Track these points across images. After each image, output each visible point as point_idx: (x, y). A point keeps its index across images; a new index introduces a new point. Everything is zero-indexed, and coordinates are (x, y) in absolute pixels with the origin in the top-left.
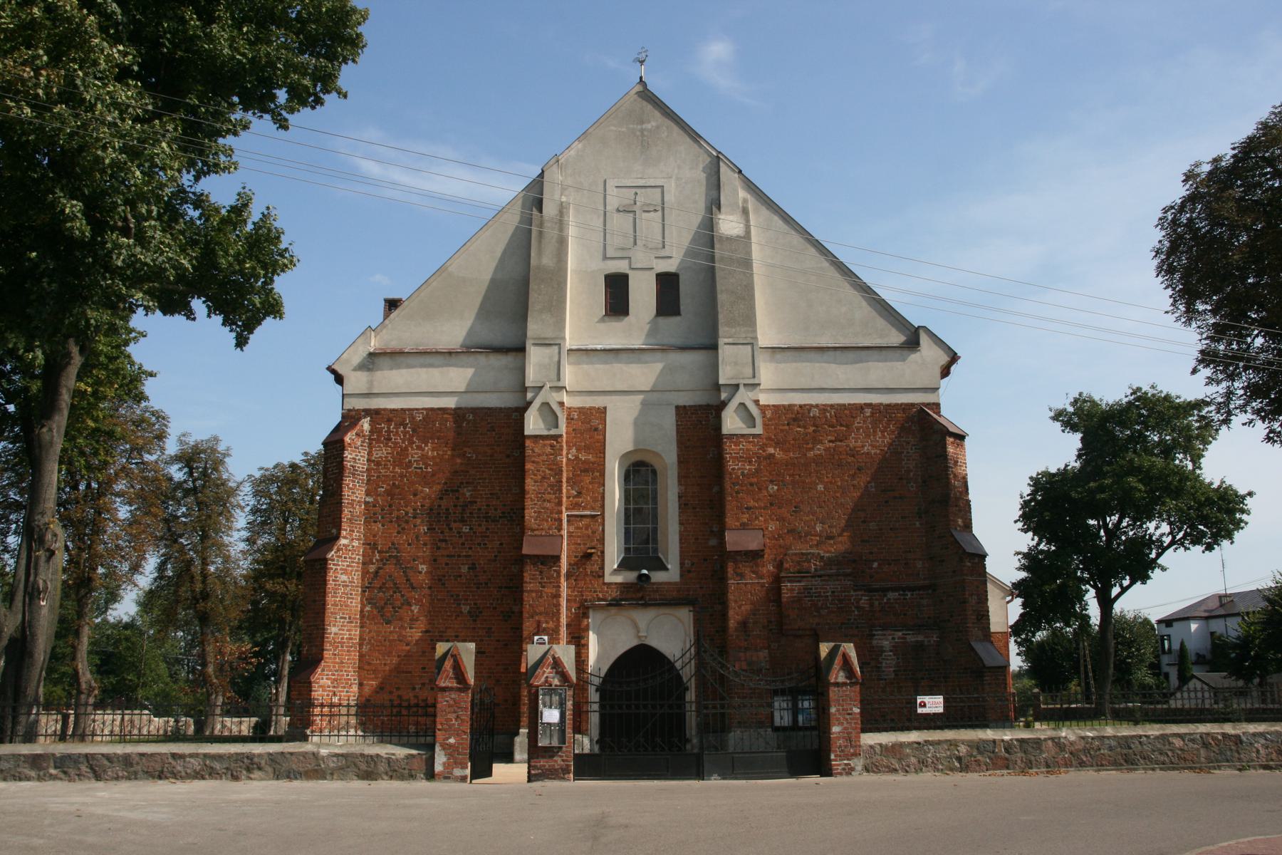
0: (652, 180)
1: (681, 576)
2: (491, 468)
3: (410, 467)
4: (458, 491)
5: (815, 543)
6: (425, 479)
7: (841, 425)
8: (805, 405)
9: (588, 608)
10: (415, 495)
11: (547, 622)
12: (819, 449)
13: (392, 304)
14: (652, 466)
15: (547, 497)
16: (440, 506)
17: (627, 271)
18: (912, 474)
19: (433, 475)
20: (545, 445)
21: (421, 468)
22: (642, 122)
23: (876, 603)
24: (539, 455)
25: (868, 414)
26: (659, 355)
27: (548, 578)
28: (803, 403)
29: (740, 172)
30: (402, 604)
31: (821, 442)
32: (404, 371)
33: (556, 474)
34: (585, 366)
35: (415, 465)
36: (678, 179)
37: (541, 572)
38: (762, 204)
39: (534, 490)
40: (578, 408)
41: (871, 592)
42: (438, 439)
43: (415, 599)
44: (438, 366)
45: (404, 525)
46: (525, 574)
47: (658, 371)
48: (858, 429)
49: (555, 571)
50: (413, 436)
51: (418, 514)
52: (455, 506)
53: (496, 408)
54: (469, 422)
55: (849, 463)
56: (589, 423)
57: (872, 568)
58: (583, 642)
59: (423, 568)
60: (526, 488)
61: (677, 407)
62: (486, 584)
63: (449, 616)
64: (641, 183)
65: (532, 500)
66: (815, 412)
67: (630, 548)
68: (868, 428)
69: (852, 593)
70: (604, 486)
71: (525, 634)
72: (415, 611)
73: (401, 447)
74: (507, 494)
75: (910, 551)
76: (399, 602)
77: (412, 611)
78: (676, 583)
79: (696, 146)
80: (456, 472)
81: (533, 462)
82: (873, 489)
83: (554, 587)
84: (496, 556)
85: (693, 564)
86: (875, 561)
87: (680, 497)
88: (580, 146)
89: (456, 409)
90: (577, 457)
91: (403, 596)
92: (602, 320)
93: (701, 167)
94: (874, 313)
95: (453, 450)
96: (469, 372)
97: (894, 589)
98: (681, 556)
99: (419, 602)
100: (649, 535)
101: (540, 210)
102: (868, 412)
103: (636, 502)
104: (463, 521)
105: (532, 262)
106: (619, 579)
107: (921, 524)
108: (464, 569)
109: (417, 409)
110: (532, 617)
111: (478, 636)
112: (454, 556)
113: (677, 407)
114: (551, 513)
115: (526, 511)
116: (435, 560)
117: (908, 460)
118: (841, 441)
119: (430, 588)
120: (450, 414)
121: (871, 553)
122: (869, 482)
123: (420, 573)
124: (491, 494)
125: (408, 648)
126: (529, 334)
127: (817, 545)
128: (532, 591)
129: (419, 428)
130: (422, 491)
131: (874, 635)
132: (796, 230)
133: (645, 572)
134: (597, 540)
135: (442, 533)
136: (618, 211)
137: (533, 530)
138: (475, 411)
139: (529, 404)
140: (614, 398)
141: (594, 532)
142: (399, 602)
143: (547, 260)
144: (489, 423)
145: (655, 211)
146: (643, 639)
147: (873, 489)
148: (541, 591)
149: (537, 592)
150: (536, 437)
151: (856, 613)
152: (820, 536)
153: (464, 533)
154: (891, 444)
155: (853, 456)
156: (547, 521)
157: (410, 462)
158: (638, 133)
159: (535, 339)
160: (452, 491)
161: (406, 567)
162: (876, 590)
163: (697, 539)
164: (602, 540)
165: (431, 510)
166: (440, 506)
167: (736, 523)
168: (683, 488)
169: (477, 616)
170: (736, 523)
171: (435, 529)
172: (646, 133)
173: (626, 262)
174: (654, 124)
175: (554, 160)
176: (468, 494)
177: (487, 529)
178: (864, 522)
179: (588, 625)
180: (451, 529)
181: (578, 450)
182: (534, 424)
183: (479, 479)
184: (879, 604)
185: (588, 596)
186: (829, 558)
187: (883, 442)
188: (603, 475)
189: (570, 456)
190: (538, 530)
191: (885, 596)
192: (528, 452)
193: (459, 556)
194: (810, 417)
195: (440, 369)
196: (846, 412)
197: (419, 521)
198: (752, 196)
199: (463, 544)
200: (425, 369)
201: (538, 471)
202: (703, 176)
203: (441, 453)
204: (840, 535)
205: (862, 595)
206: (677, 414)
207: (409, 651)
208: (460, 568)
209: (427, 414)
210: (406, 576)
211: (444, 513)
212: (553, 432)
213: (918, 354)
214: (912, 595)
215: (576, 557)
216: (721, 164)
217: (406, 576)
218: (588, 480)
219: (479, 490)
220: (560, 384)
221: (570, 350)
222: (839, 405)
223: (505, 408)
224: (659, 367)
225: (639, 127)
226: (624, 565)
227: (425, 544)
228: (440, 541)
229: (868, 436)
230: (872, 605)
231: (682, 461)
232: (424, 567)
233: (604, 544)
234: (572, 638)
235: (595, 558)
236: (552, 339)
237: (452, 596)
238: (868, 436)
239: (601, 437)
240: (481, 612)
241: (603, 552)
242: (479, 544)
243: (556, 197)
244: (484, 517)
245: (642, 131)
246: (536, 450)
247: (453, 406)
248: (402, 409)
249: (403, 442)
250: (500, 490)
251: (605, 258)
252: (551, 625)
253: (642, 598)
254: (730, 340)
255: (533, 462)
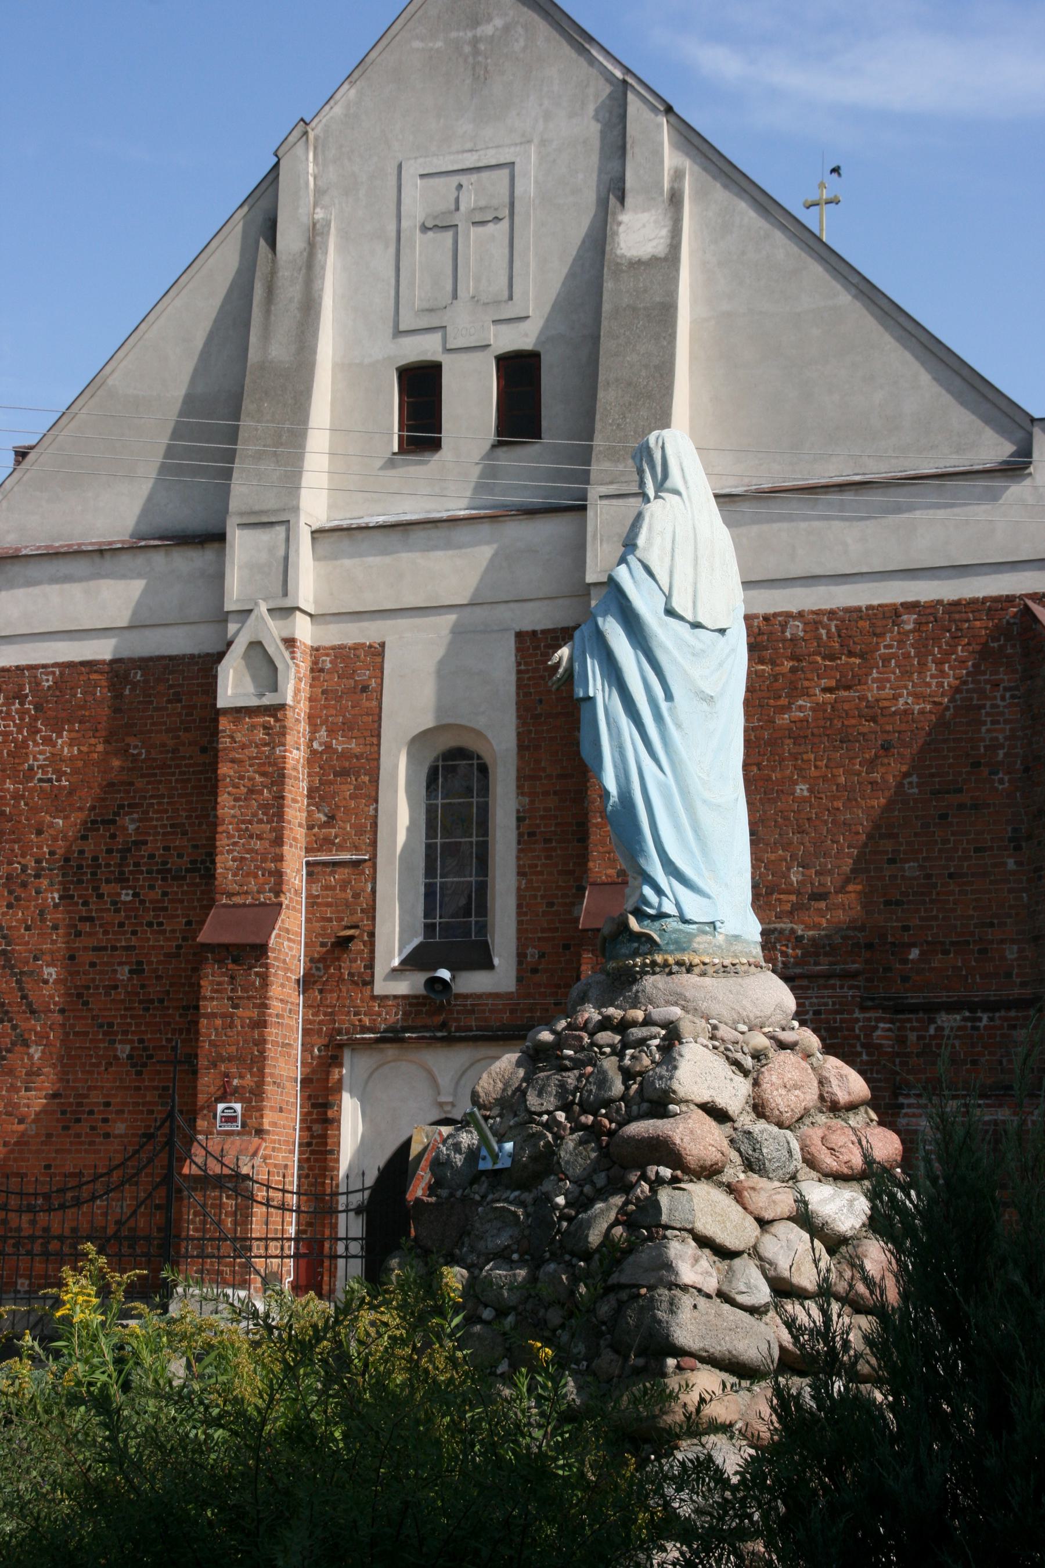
0: (492, 152)
1: (520, 980)
2: (173, 774)
3: (32, 779)
4: (114, 822)
5: (788, 907)
6: (57, 801)
7: (851, 654)
8: (775, 615)
9: (340, 1046)
10: (39, 832)
11: (242, 1077)
12: (801, 708)
13: (21, 455)
14: (479, 757)
15: (256, 828)
16: (81, 852)
17: (439, 357)
18: (1001, 753)
19: (71, 792)
20: (253, 727)
21: (50, 780)
22: (475, 22)
23: (912, 1037)
24: (243, 747)
25: (910, 627)
26: (485, 528)
27: (245, 990)
28: (772, 611)
29: (669, 110)
30: (14, 1044)
31: (806, 693)
32: (20, 593)
33: (273, 783)
34: (347, 562)
35: (39, 776)
36: (543, 143)
37: (232, 978)
38: (715, 178)
39: (234, 816)
40: (333, 648)
41: (902, 1012)
42: (80, 723)
43: (36, 1033)
44: (80, 580)
45: (19, 891)
46: (202, 983)
47: (485, 564)
48: (886, 660)
49: (257, 974)
50: (35, 719)
51: (43, 869)
52: (109, 851)
53: (184, 656)
54: (134, 685)
55: (864, 735)
56: (351, 676)
57: (905, 961)
58: (330, 1114)
59: (51, 973)
60: (220, 812)
61: (520, 635)
62: (161, 1001)
63: (92, 1065)
64: (470, 160)
65: (230, 836)
66: (796, 628)
67: (434, 925)
68: (907, 656)
69: (857, 1014)
70: (376, 801)
71: (202, 1098)
72: (36, 1057)
73: (15, 740)
74: (200, 824)
75: (992, 925)
76: (8, 1040)
77: (31, 1057)
78: (508, 995)
79: (582, 62)
80: (111, 785)
81: (233, 761)
82: (915, 790)
83: (255, 1006)
84: (179, 947)
85: (542, 955)
86: (914, 945)
87: (520, 819)
88: (353, 92)
89: (113, 662)
90: (328, 747)
91: (14, 1027)
92: (390, 463)
93: (591, 109)
94: (947, 398)
95: (107, 741)
96: (137, 586)
97: (952, 1008)
98: (519, 939)
99: (42, 1037)
100: (470, 897)
101: (273, 244)
102: (909, 621)
103: (447, 832)
104: (122, 880)
105: (250, 356)
106: (402, 987)
107: (1019, 863)
108: (123, 973)
109: (44, 666)
110: (215, 1066)
111: (144, 1104)
112: (105, 948)
113: (520, 635)
114: (264, 860)
115: (219, 859)
116: (72, 958)
117: (993, 723)
118: (848, 688)
119: (62, 1011)
120: (102, 673)
121: (906, 928)
122: (906, 775)
123: (46, 982)
124: (172, 826)
125: (22, 1127)
126: (234, 505)
127: (791, 913)
128: (214, 1015)
129: (47, 702)
130: (51, 825)
131: (901, 1106)
132: (783, 227)
133: (445, 974)
134: (362, 911)
135: (85, 904)
136: (425, 229)
137: (230, 895)
138: (145, 663)
139: (230, 644)
140: (403, 623)
141: (356, 896)
142: (8, 1040)
143: (279, 351)
144: (171, 687)
145: (497, 219)
146: (448, 1108)
147: (915, 790)
148: (232, 1015)
149: (224, 1016)
150: (238, 710)
151: (865, 1057)
152: (799, 893)
153: (125, 903)
154: (957, 690)
155: (873, 719)
156: (256, 876)
157: (31, 768)
158: (467, 49)
159: (241, 514)
160: (103, 822)
161: (22, 973)
162: (913, 1009)
163: (551, 904)
164: (371, 912)
165: (67, 860)
166: (81, 852)
167: (610, 871)
168: (527, 800)
169: (145, 1065)
170: (610, 871)
171: (72, 897)
172: (482, 47)
173: (437, 337)
174: (498, 22)
175: (296, 133)
176: (132, 827)
177: (165, 894)
178: (892, 861)
179: (340, 1080)
180: (100, 896)
181: (331, 732)
182: (235, 686)
183: (152, 797)
184: (919, 1038)
185: (344, 1021)
186: (813, 939)
187: (940, 685)
188: (375, 780)
189: (315, 745)
190: (238, 894)
191: (932, 1021)
192: (225, 742)
193: (114, 948)
194: (784, 640)
195: (84, 584)
196: (861, 623)
197: (45, 883)
198: (694, 160)
199: (121, 925)
200: (56, 587)
201: (242, 778)
202: (595, 128)
203: (84, 749)
204: (841, 890)
205: (878, 1020)
206: (518, 650)
207: (23, 1134)
208: (115, 971)
209: (62, 674)
210: (21, 989)
211: (88, 866)
212: (268, 700)
213: (1027, 482)
214: (991, 1019)
215: (323, 945)
216: (631, 96)
217: (21, 989)
218: (347, 790)
219: (152, 819)
220: (288, 603)
221: (317, 534)
222: (848, 610)
223: (199, 656)
224: (485, 553)
225: (470, 34)
226: (414, 961)
227: (55, 927)
228: (82, 919)
229: (906, 674)
230: (902, 1040)
231: (525, 745)
232: (52, 970)
233: (373, 919)
234: (314, 1106)
235: (356, 946)
236: (275, 511)
237: (101, 1026)
238: (906, 674)
239: (374, 703)
240: (150, 1057)
241: (372, 935)
242: (150, 924)
243: (303, 211)
244: (158, 872)
245: (475, 41)
246: (239, 737)
247: (108, 656)
248: (18, 667)
249: (20, 732)
250: (189, 817)
251: (398, 333)
252: (249, 1080)
253: (444, 1026)
254: (612, 489)
255: (233, 761)
